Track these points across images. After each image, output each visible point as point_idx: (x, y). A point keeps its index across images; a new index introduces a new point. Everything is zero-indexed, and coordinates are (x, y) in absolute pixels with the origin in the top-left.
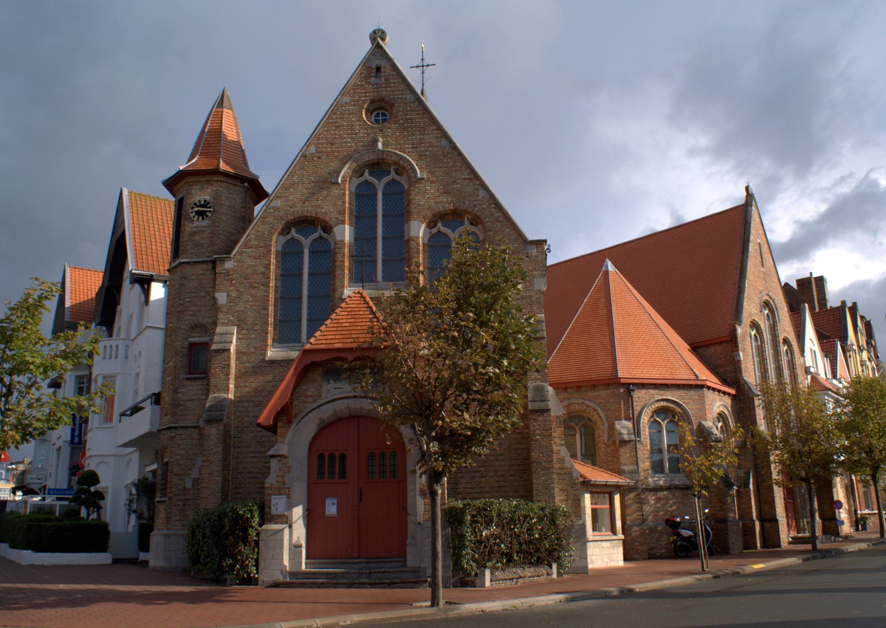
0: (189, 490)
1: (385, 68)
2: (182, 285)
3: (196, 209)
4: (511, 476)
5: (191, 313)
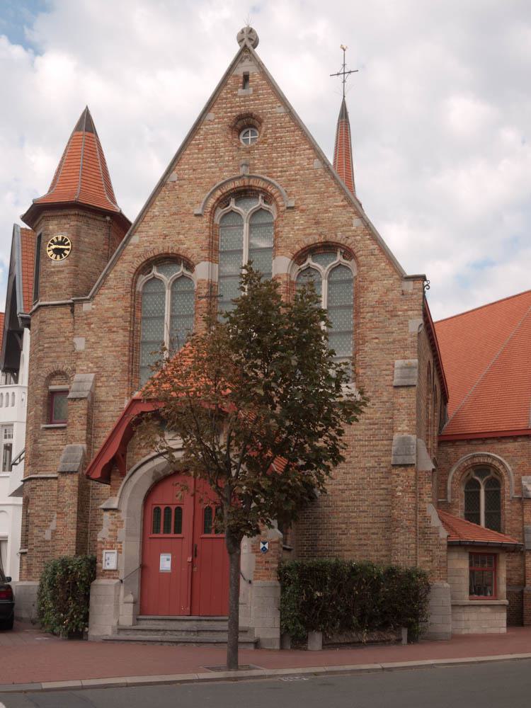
0: (48, 541)
1: (253, 76)
3: (54, 247)
4: (373, 534)
5: (51, 359)
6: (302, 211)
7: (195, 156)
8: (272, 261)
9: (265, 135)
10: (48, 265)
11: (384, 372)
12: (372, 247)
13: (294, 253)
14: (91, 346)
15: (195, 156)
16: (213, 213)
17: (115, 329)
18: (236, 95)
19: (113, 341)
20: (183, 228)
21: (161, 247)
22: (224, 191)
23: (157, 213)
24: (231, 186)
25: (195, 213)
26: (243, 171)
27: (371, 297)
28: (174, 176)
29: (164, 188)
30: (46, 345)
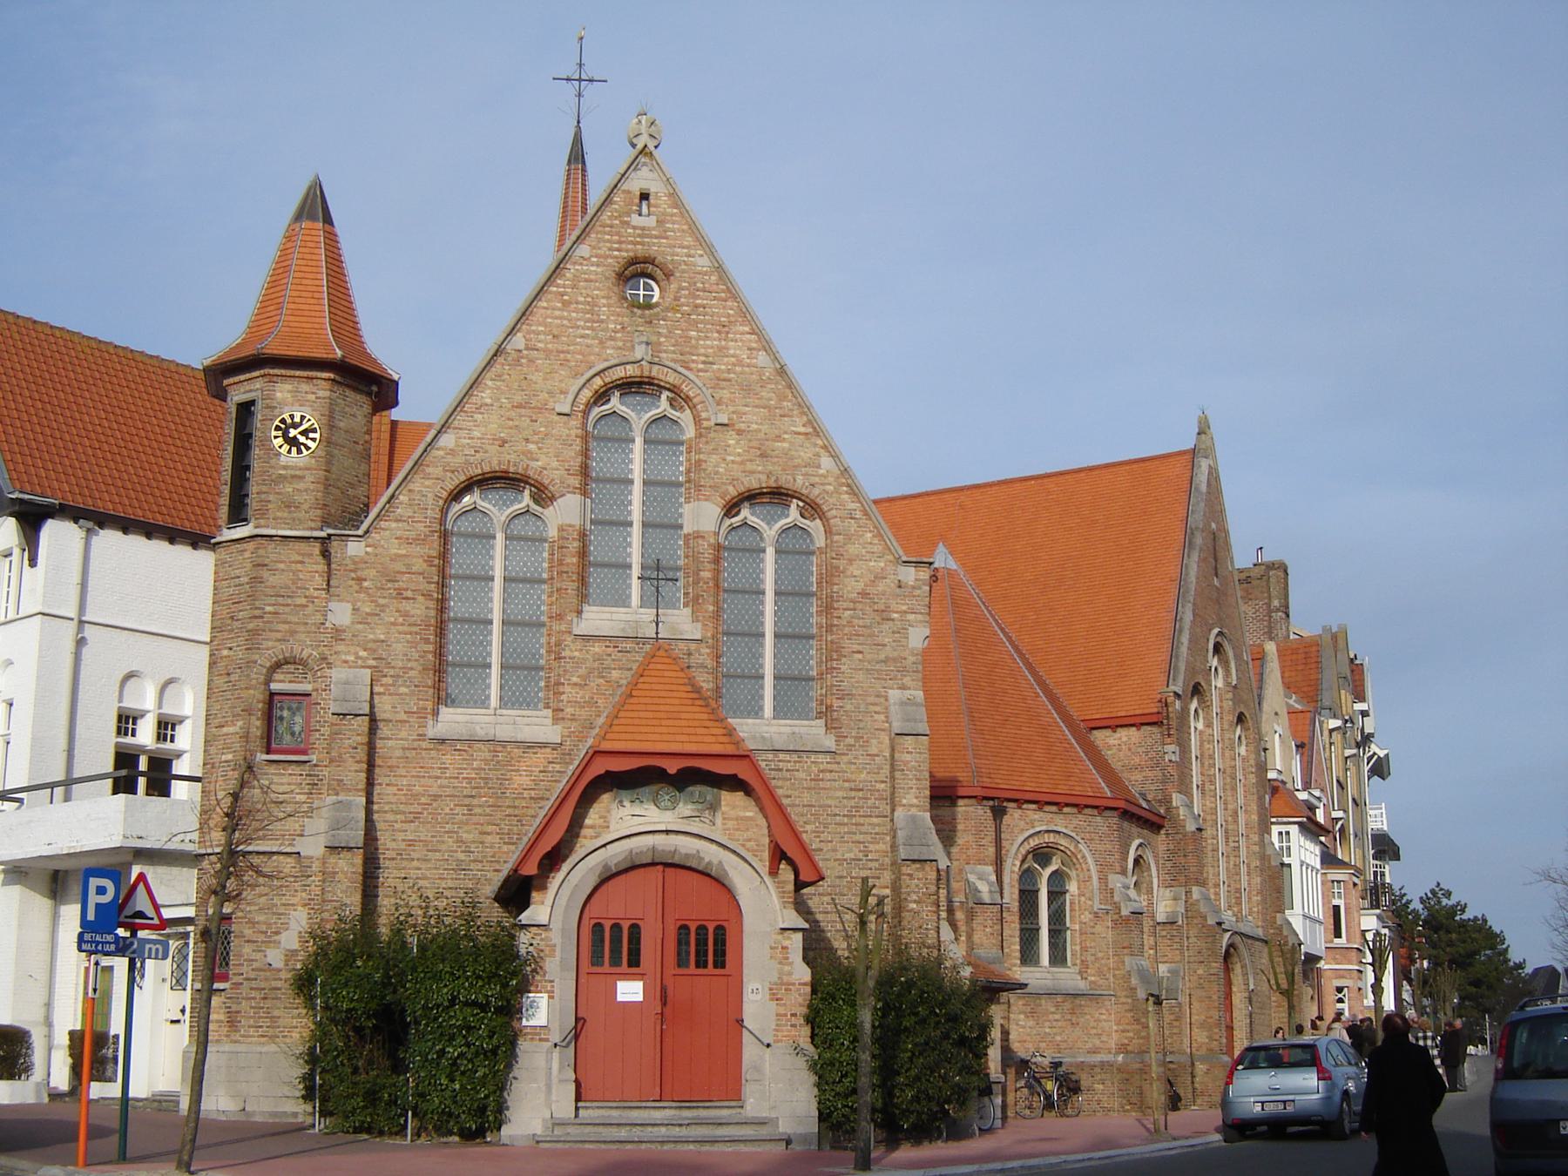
1: (657, 198)
2: (256, 580)
5: (279, 635)
6: (740, 432)
7: (557, 313)
8: (681, 505)
9: (676, 299)
10: (273, 462)
11: (872, 708)
12: (853, 506)
13: (728, 498)
14: (363, 619)
15: (557, 313)
16: (586, 413)
17: (409, 594)
18: (627, 223)
19: (406, 615)
20: (535, 433)
21: (494, 460)
22: (608, 380)
23: (488, 401)
24: (619, 373)
25: (558, 410)
26: (639, 352)
27: (850, 586)
28: (519, 341)
29: (500, 360)
30: (268, 609)
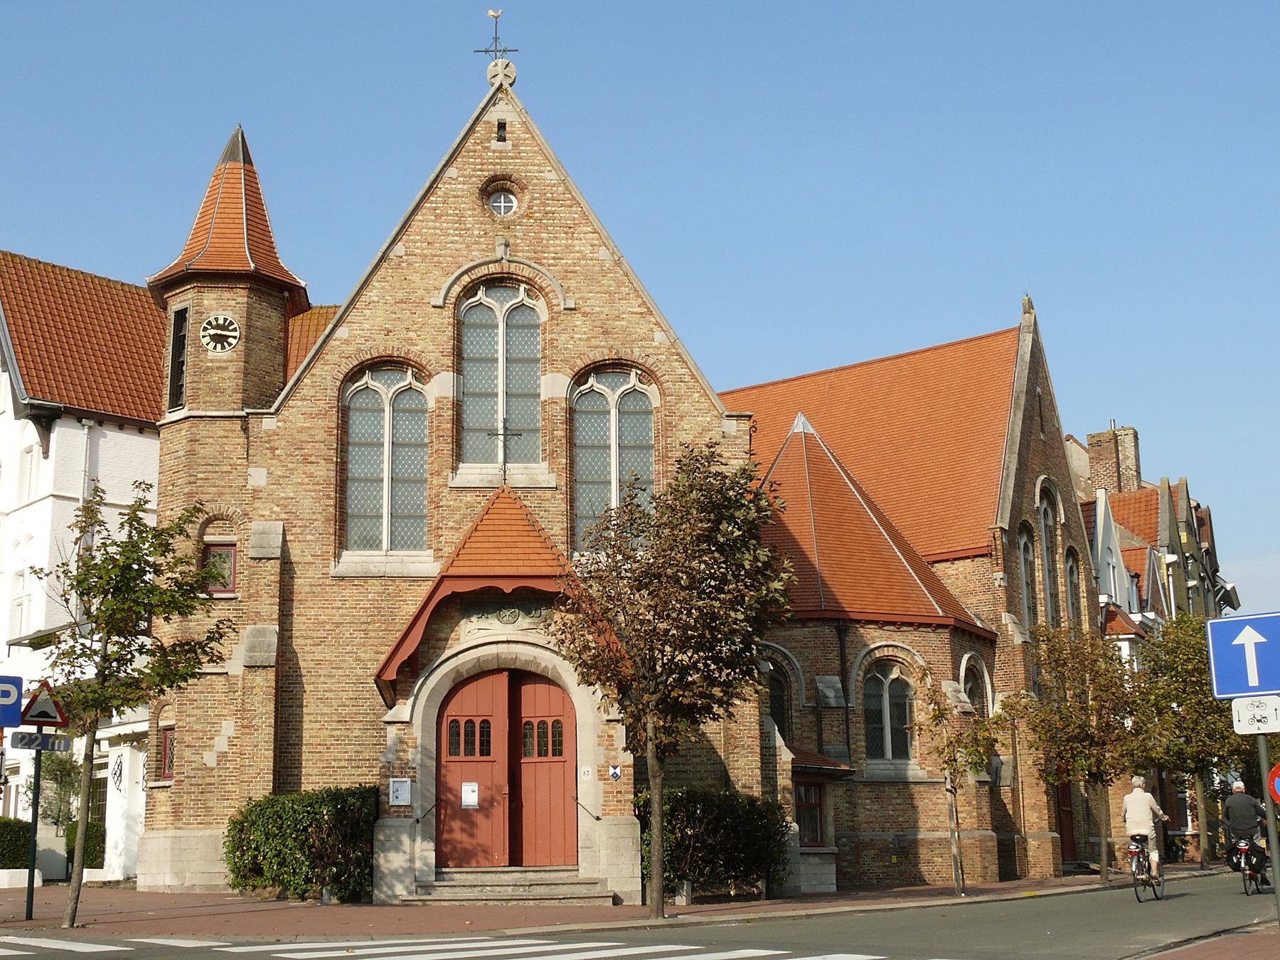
0: (213, 769)
1: (512, 126)
2: (191, 453)
3: (213, 332)
4: (695, 756)
6: (585, 314)
8: (539, 378)
14: (277, 481)
17: (313, 459)
18: (488, 148)
19: (311, 476)
21: (381, 346)
22: (474, 277)
23: (376, 299)
24: (484, 271)
26: (500, 252)
28: (400, 249)
29: (385, 265)
30: (200, 475)
